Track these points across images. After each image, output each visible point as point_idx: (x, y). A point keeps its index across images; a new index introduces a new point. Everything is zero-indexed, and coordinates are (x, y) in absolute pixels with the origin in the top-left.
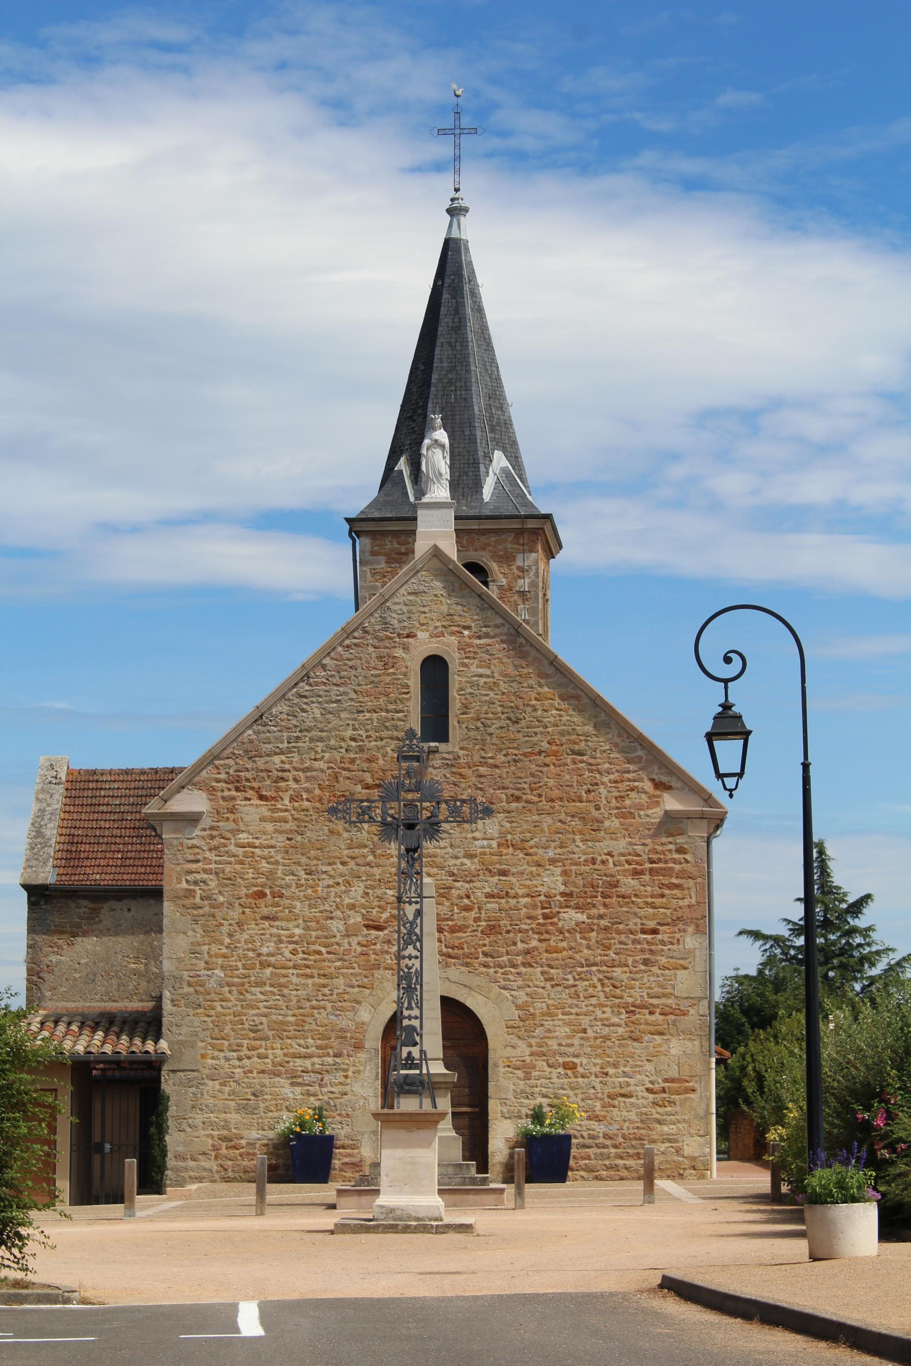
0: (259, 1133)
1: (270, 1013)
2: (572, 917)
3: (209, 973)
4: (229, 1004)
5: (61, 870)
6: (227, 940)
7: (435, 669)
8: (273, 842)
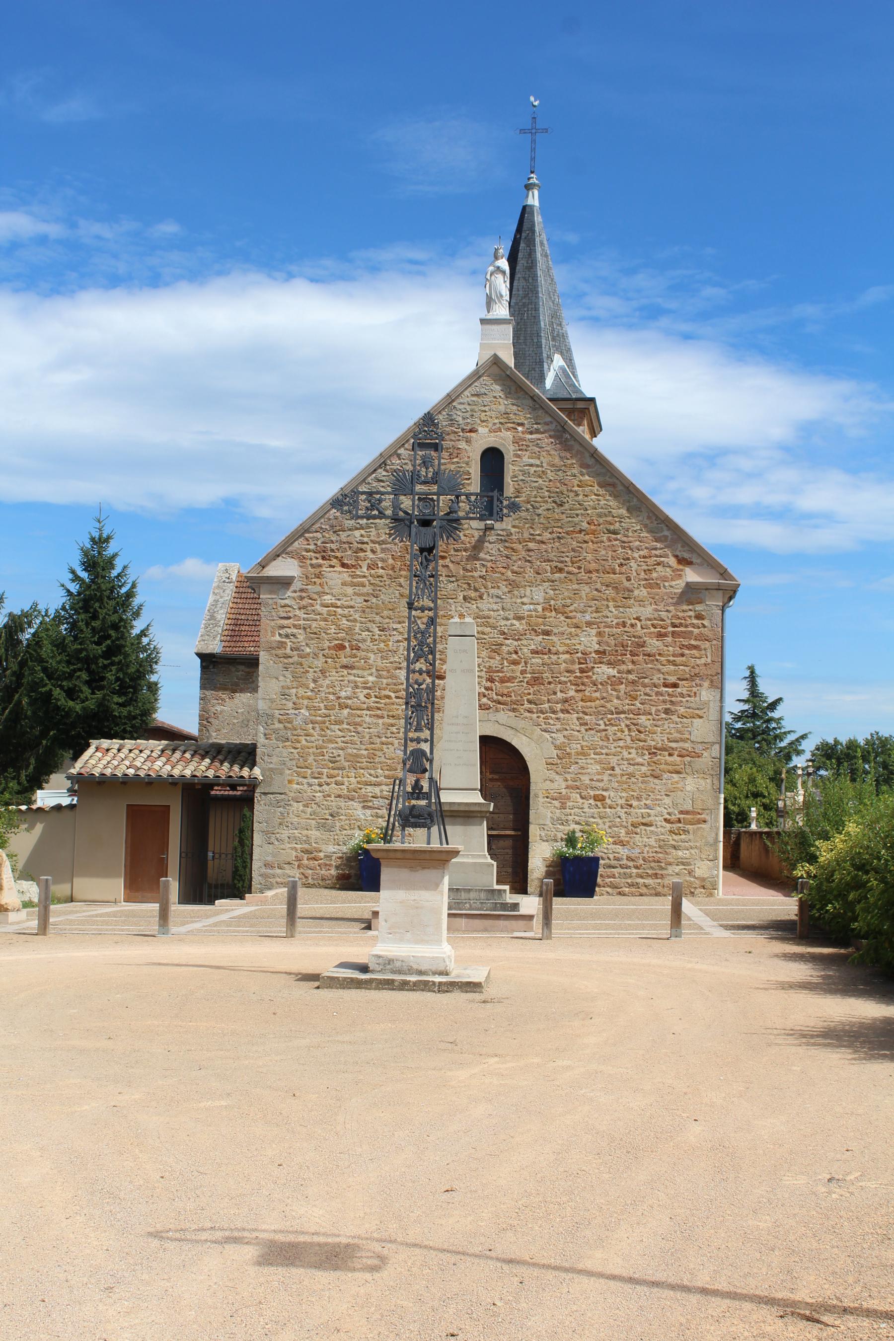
0: (335, 848)
1: (347, 748)
2: (604, 671)
3: (296, 712)
4: (313, 739)
5: (226, 644)
6: (312, 685)
7: (493, 459)
8: (352, 603)
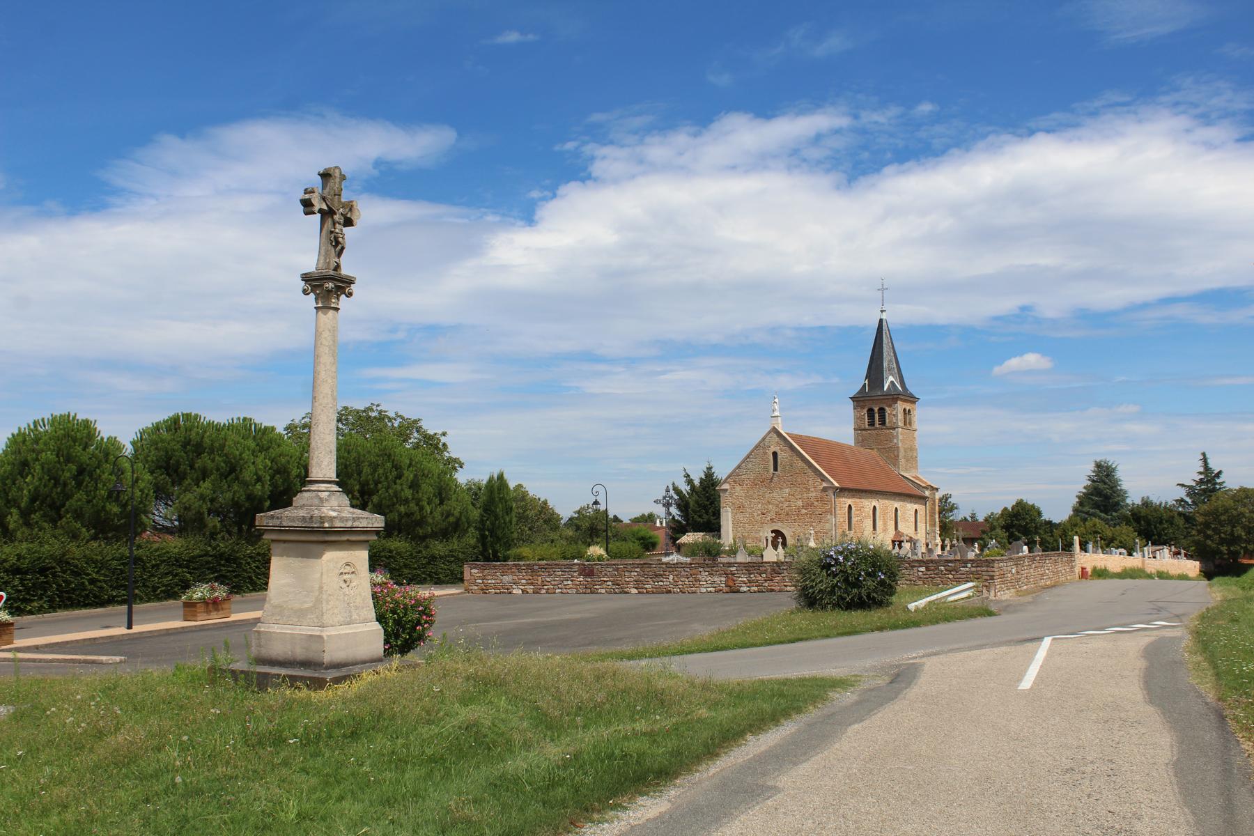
7: (775, 454)
